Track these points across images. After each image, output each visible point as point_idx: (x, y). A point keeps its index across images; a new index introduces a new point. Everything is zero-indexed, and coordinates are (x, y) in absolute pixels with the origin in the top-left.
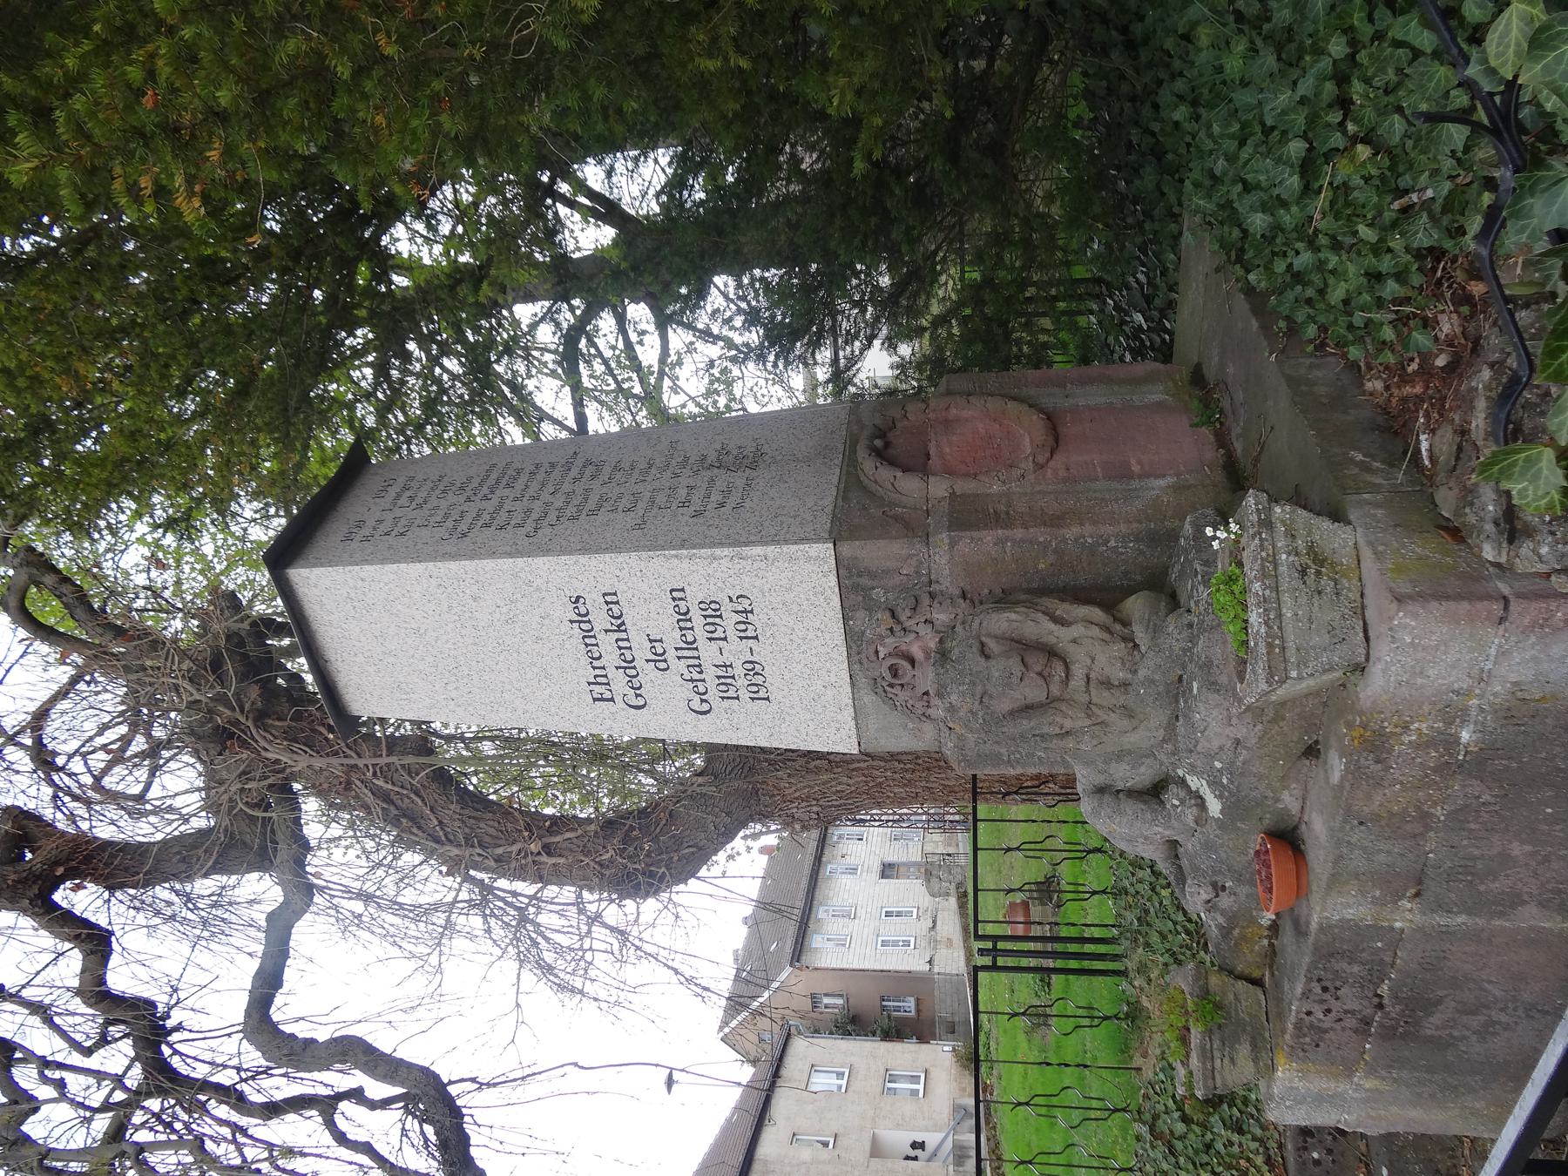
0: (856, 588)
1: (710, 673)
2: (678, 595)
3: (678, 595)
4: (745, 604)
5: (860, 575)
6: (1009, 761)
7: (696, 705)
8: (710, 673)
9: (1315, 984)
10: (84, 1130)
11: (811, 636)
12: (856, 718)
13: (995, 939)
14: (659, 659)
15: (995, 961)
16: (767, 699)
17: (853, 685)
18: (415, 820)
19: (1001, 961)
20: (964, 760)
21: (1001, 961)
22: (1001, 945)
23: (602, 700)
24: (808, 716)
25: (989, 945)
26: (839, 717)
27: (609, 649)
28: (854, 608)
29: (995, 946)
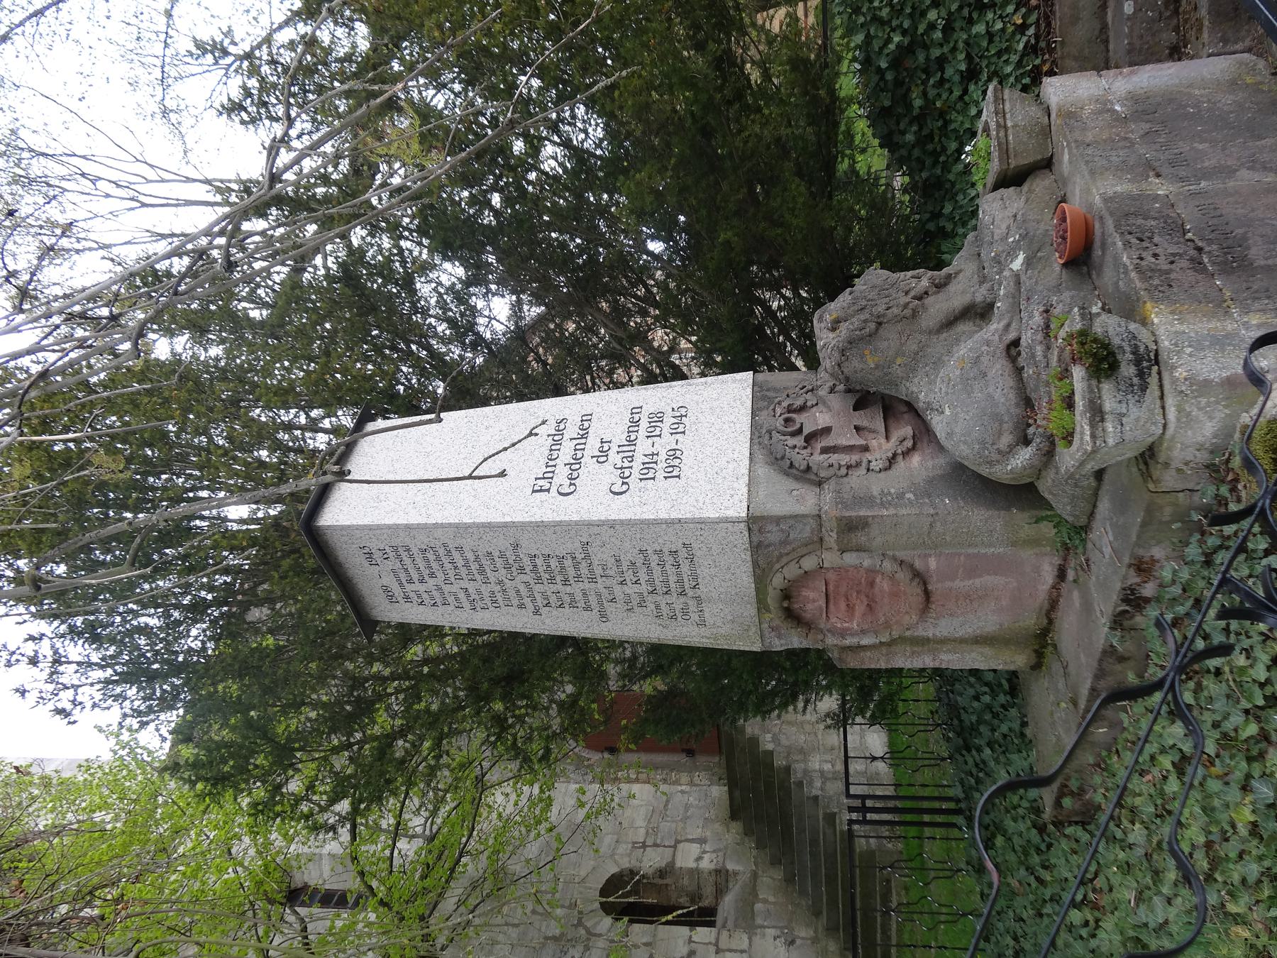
0: (764, 398)
1: (639, 459)
2: (603, 616)
3: (603, 616)
4: (683, 411)
5: (768, 390)
6: (882, 503)
7: (616, 488)
8: (639, 459)
9: (1129, 237)
10: (171, 115)
11: (726, 426)
12: (749, 485)
13: (863, 798)
14: (604, 453)
15: (864, 817)
16: (678, 477)
17: (751, 459)
18: (387, 411)
19: (869, 816)
20: (842, 503)
21: (869, 816)
22: (869, 803)
23: (541, 491)
24: (709, 487)
25: (857, 803)
26: (736, 485)
27: (567, 451)
28: (760, 409)
29: (863, 804)
